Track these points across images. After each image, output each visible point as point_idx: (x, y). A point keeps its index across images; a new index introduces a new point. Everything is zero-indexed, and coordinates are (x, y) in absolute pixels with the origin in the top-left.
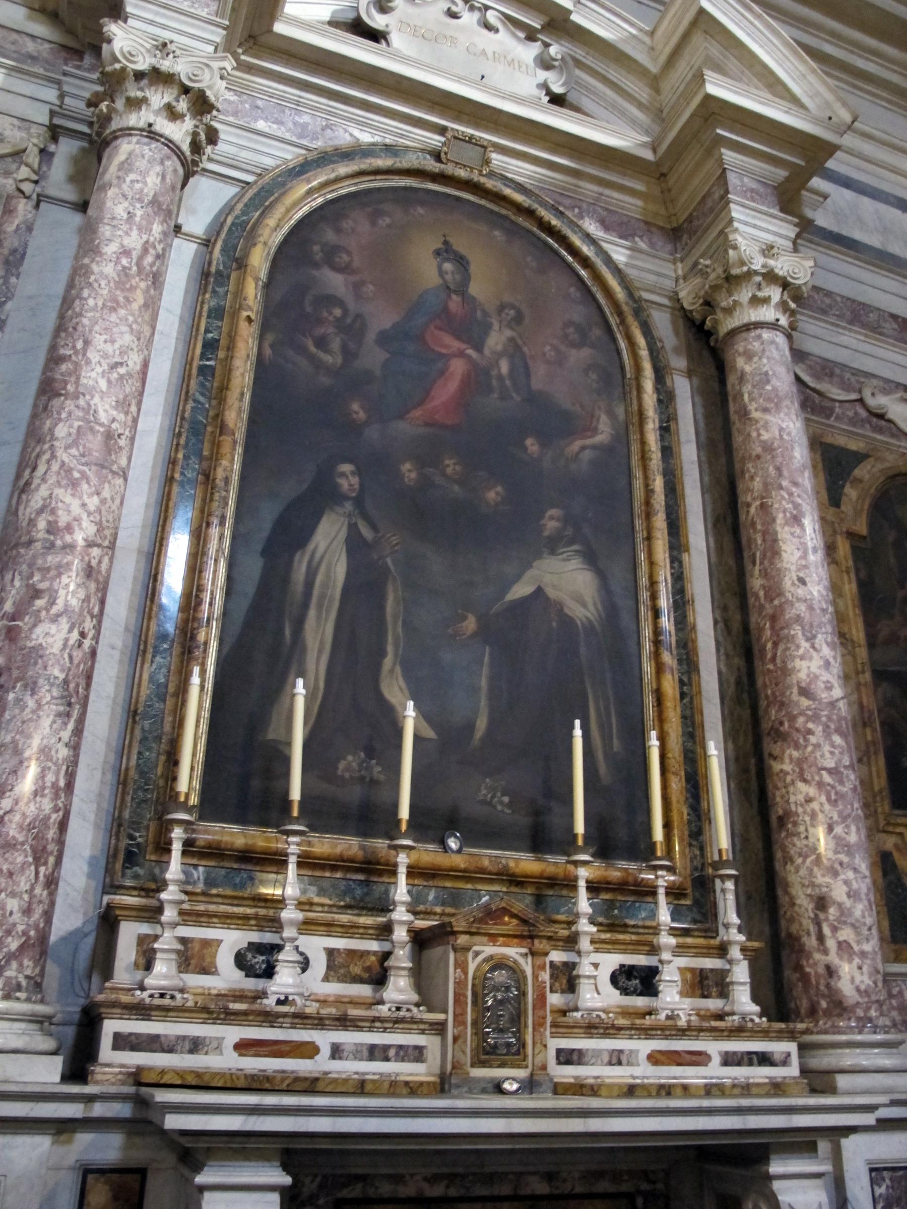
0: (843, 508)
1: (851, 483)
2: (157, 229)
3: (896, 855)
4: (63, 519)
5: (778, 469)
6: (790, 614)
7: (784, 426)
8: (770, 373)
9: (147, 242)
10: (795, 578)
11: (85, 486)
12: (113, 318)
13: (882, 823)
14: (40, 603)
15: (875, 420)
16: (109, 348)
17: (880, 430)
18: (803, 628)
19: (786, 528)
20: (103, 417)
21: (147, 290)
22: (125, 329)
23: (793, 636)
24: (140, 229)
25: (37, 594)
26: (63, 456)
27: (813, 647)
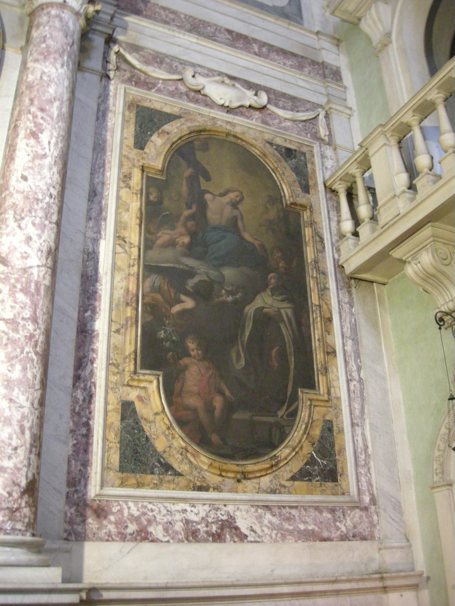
0: (146, 150)
1: (159, 134)
3: (138, 405)
5: (32, 101)
6: (9, 202)
7: (46, 70)
8: (48, 36)
10: (20, 176)
13: (127, 378)
15: (193, 94)
17: (197, 101)
18: (15, 213)
19: (25, 141)
23: (6, 219)
27: (20, 227)
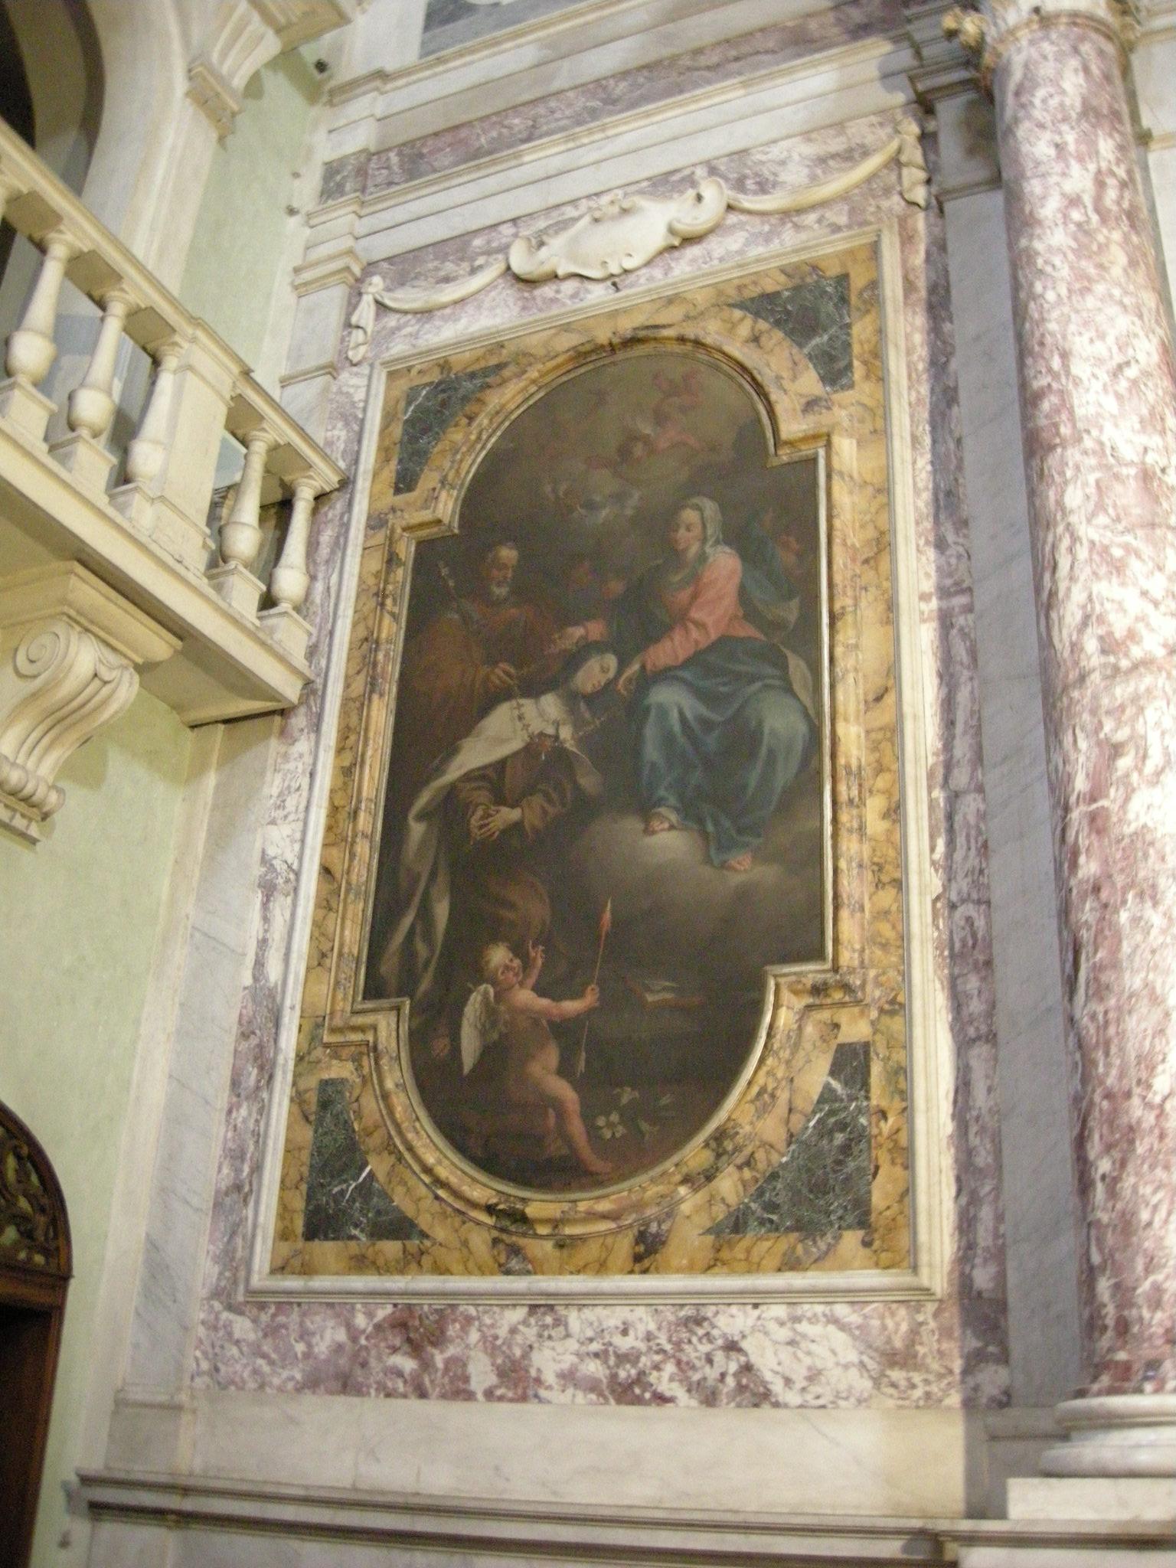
2: (1106, 147)
4: (1119, 626)
9: (1099, 172)
11: (1134, 563)
12: (1090, 302)
14: (1124, 763)
16: (1100, 349)
20: (1128, 453)
21: (1126, 238)
22: (1113, 310)
24: (1081, 160)
25: (1116, 750)
26: (1086, 532)
